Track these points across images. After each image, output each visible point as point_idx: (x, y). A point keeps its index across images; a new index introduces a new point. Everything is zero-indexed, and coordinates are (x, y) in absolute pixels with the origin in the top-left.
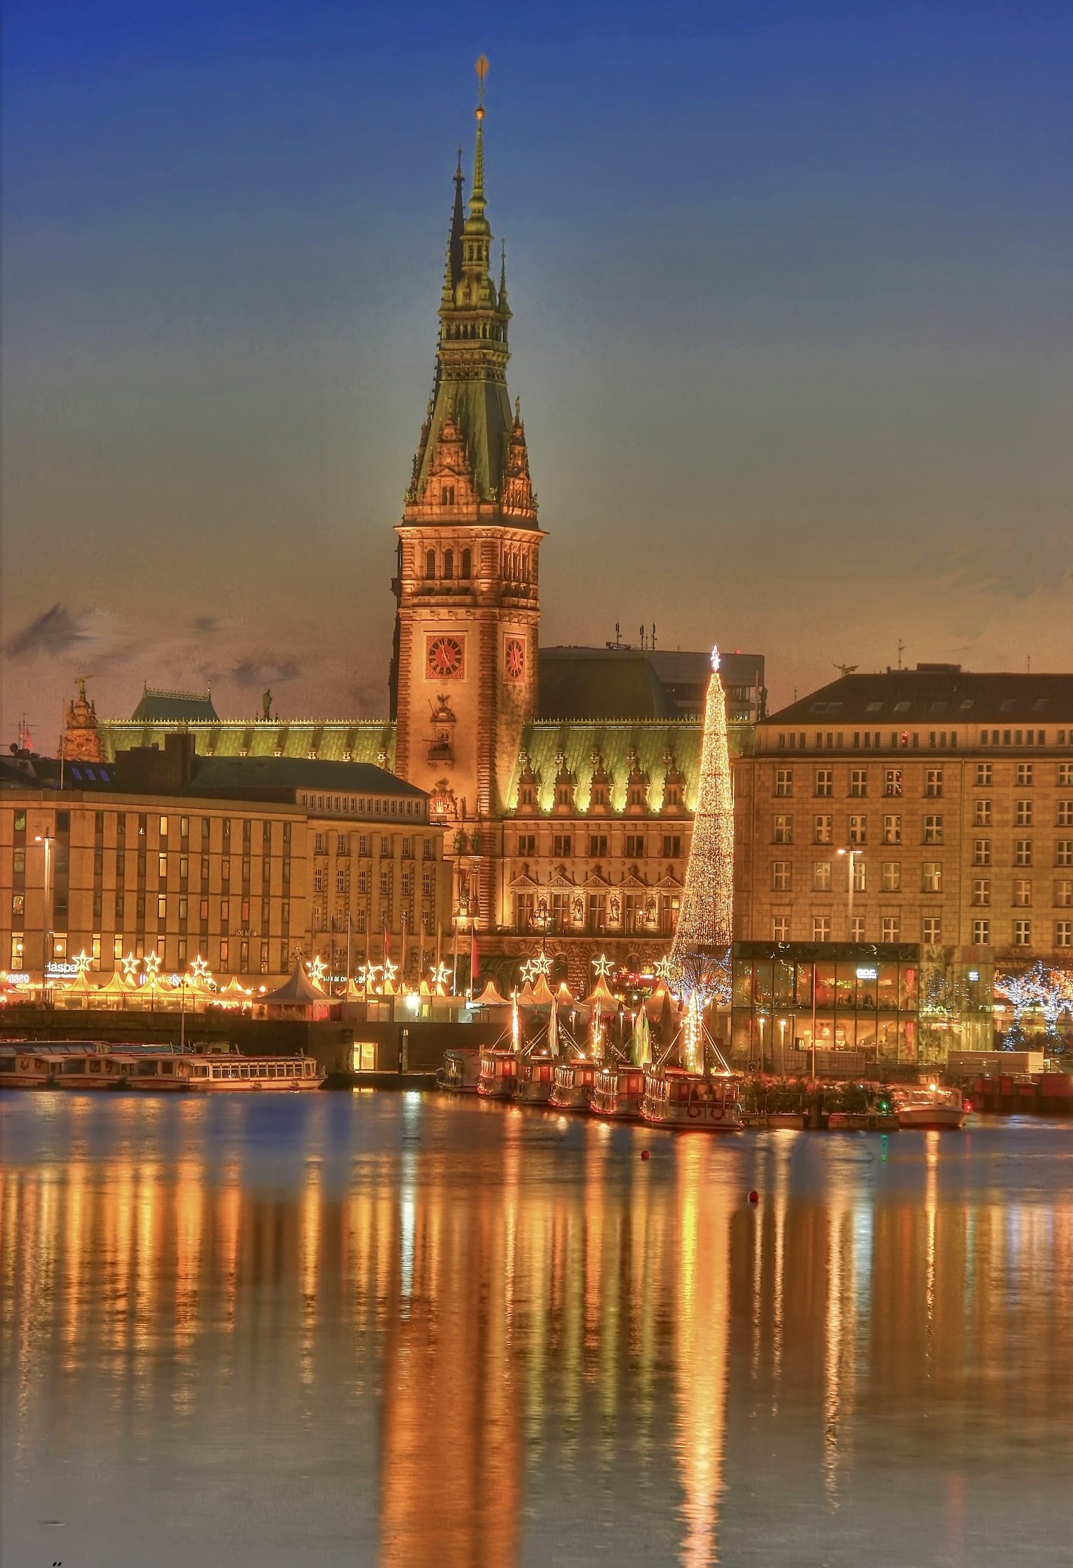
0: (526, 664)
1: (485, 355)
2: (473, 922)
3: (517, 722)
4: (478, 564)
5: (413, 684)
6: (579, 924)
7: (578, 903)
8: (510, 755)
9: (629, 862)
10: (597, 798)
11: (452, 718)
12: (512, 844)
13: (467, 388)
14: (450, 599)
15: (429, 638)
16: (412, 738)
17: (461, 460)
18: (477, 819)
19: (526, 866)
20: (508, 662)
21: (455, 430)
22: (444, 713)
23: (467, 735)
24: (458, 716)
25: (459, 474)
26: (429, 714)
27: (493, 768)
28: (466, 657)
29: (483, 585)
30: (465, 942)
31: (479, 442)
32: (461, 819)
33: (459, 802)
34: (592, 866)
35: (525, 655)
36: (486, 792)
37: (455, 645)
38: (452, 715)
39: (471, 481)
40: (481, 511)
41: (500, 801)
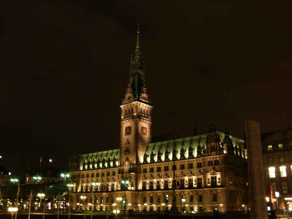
0: (148, 133)
1: (137, 71)
2: (131, 188)
3: (145, 145)
4: (135, 110)
5: (123, 137)
7: (155, 183)
8: (143, 151)
11: (129, 143)
12: (142, 170)
14: (128, 118)
15: (126, 127)
16: (122, 149)
20: (142, 131)
22: (128, 142)
23: (132, 146)
25: (131, 93)
29: (135, 114)
30: (129, 193)
34: (157, 174)
35: (147, 131)
36: (135, 158)
39: (133, 94)
41: (139, 161)
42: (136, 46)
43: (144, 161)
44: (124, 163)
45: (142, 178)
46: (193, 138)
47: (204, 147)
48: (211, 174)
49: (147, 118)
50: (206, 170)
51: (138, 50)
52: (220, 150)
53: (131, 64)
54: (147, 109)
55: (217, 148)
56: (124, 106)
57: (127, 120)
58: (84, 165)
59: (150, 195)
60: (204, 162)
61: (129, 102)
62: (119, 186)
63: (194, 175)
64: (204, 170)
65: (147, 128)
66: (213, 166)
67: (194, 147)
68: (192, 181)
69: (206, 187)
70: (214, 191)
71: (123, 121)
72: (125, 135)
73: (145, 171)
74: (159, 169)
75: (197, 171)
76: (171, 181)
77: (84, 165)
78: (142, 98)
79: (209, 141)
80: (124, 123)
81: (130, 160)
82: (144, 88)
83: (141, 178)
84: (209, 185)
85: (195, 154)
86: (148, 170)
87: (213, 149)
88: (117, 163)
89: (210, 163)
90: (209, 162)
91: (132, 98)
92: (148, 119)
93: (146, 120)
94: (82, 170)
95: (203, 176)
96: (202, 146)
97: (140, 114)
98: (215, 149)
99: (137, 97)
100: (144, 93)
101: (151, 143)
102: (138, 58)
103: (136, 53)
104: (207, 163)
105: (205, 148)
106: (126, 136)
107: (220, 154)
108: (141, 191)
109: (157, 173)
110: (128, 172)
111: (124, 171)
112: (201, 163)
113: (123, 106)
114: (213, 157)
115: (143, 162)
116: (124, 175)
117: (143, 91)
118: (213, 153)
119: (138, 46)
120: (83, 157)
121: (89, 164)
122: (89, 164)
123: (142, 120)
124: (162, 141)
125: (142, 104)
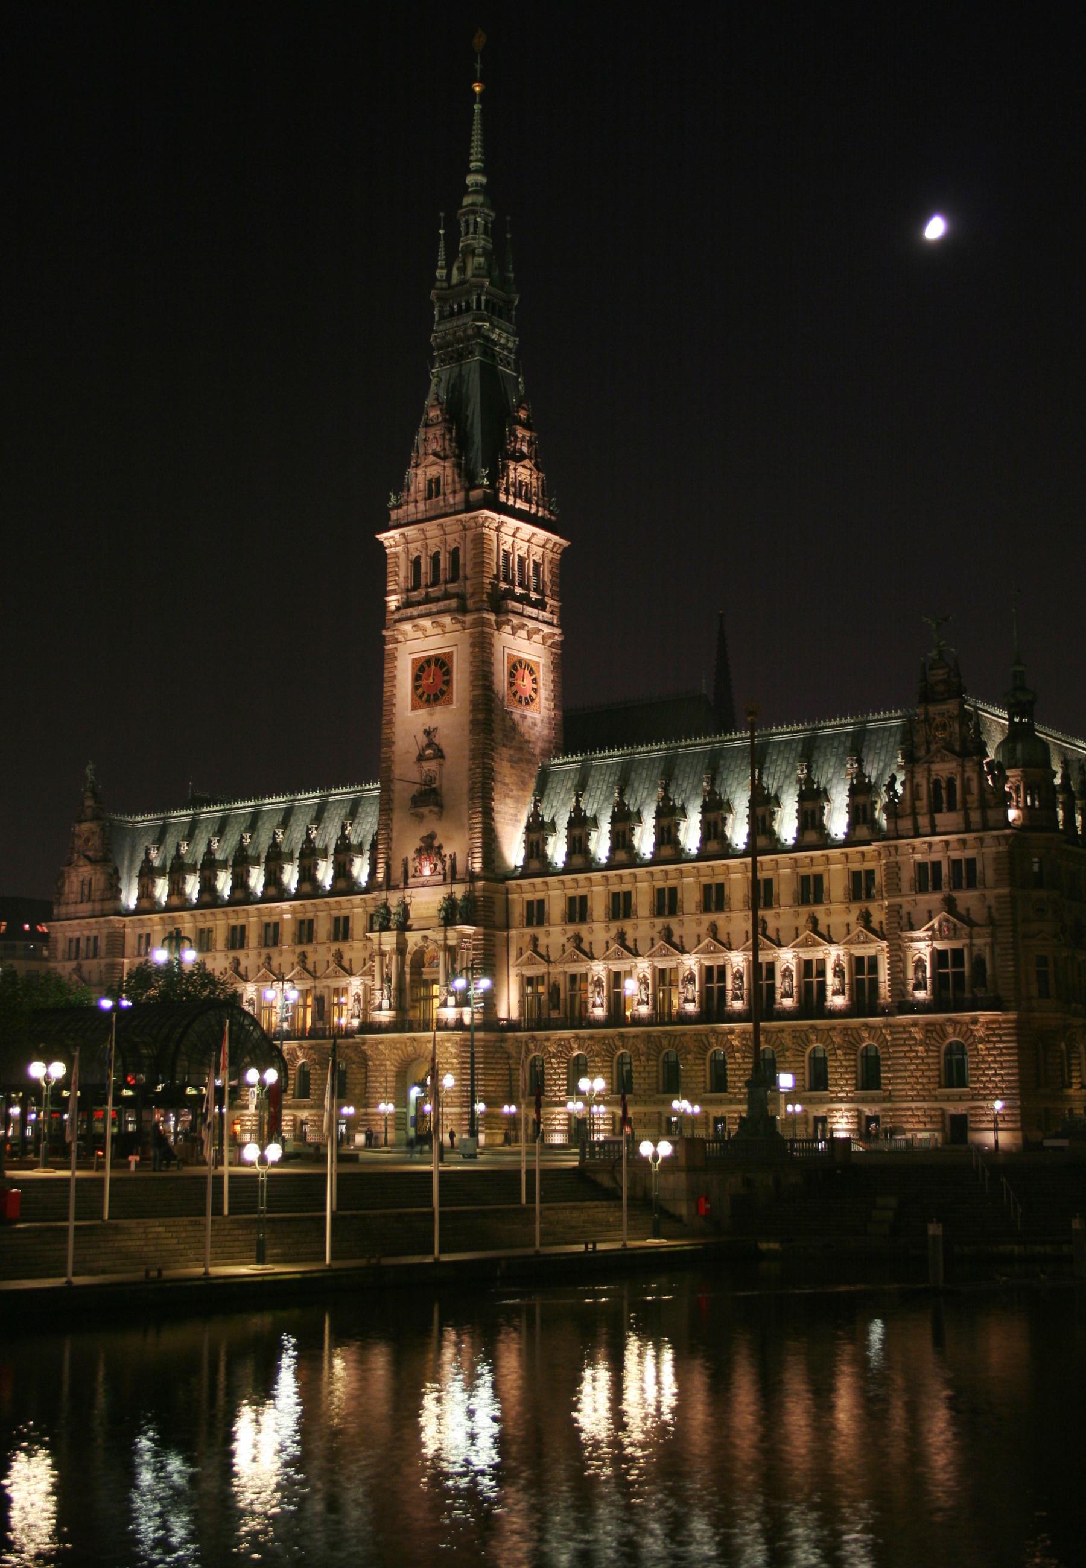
1: (479, 328)
2: (461, 1014)
3: (529, 761)
5: (398, 720)
6: (599, 1012)
7: (598, 983)
8: (517, 800)
9: (660, 922)
10: (618, 841)
11: (439, 754)
12: (518, 911)
13: (460, 370)
14: (433, 607)
15: (414, 661)
16: (397, 786)
17: (447, 443)
18: (468, 878)
19: (535, 940)
20: (512, 684)
21: (441, 410)
22: (432, 748)
24: (447, 751)
25: (444, 458)
26: (415, 752)
27: (488, 814)
28: (455, 676)
30: (448, 1040)
31: (472, 424)
32: (449, 880)
33: (447, 859)
34: (613, 933)
36: (478, 843)
37: (444, 664)
38: (440, 750)
39: (457, 465)
40: (471, 499)
42: (469, 171)
43: (528, 858)
44: (411, 871)
45: (521, 953)
46: (820, 733)
47: (891, 786)
48: (932, 938)
49: (540, 605)
50: (904, 912)
51: (480, 199)
52: (984, 806)
53: (438, 284)
54: (537, 554)
55: (966, 790)
56: (403, 535)
57: (420, 616)
58: (148, 875)
59: (572, 1049)
60: (893, 871)
61: (433, 513)
62: (385, 1004)
63: (831, 942)
64: (894, 911)
65: (538, 663)
66: (946, 889)
67: (829, 781)
68: (822, 973)
69: (906, 1006)
70: (950, 1030)
71: (396, 621)
72: (415, 707)
73: (536, 914)
74: (621, 906)
75: (853, 917)
76: (696, 970)
77: (148, 875)
78: (512, 489)
79: (922, 753)
80: (405, 634)
81: (443, 852)
82: (521, 432)
83: (513, 952)
84: (921, 995)
85: (838, 823)
86: (556, 908)
87: (942, 797)
88: (360, 869)
89: (927, 877)
90: (921, 867)
91: (448, 491)
92: (545, 615)
93: (536, 619)
94: (132, 906)
95: (884, 944)
96: (872, 772)
97: (503, 585)
98: (958, 797)
99: (486, 482)
100: (519, 458)
101: (566, 754)
102: (479, 251)
103: (464, 214)
104: (907, 874)
105: (899, 789)
106: (421, 712)
107: (985, 827)
108: (512, 1026)
109: (608, 929)
110: (436, 921)
111: (412, 914)
112: (870, 873)
113: (397, 536)
114: (947, 843)
115: (520, 863)
116: (413, 938)
117: (515, 451)
118: (944, 819)
119: (477, 171)
120: (136, 833)
121: (177, 871)
122: (177, 871)
123: (516, 620)
124: (630, 744)
125: (512, 523)
